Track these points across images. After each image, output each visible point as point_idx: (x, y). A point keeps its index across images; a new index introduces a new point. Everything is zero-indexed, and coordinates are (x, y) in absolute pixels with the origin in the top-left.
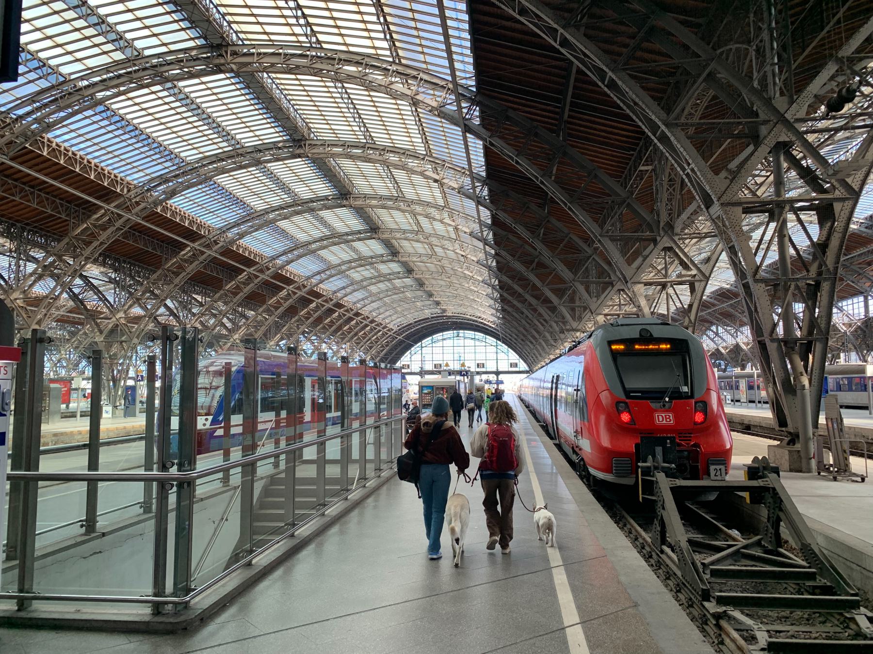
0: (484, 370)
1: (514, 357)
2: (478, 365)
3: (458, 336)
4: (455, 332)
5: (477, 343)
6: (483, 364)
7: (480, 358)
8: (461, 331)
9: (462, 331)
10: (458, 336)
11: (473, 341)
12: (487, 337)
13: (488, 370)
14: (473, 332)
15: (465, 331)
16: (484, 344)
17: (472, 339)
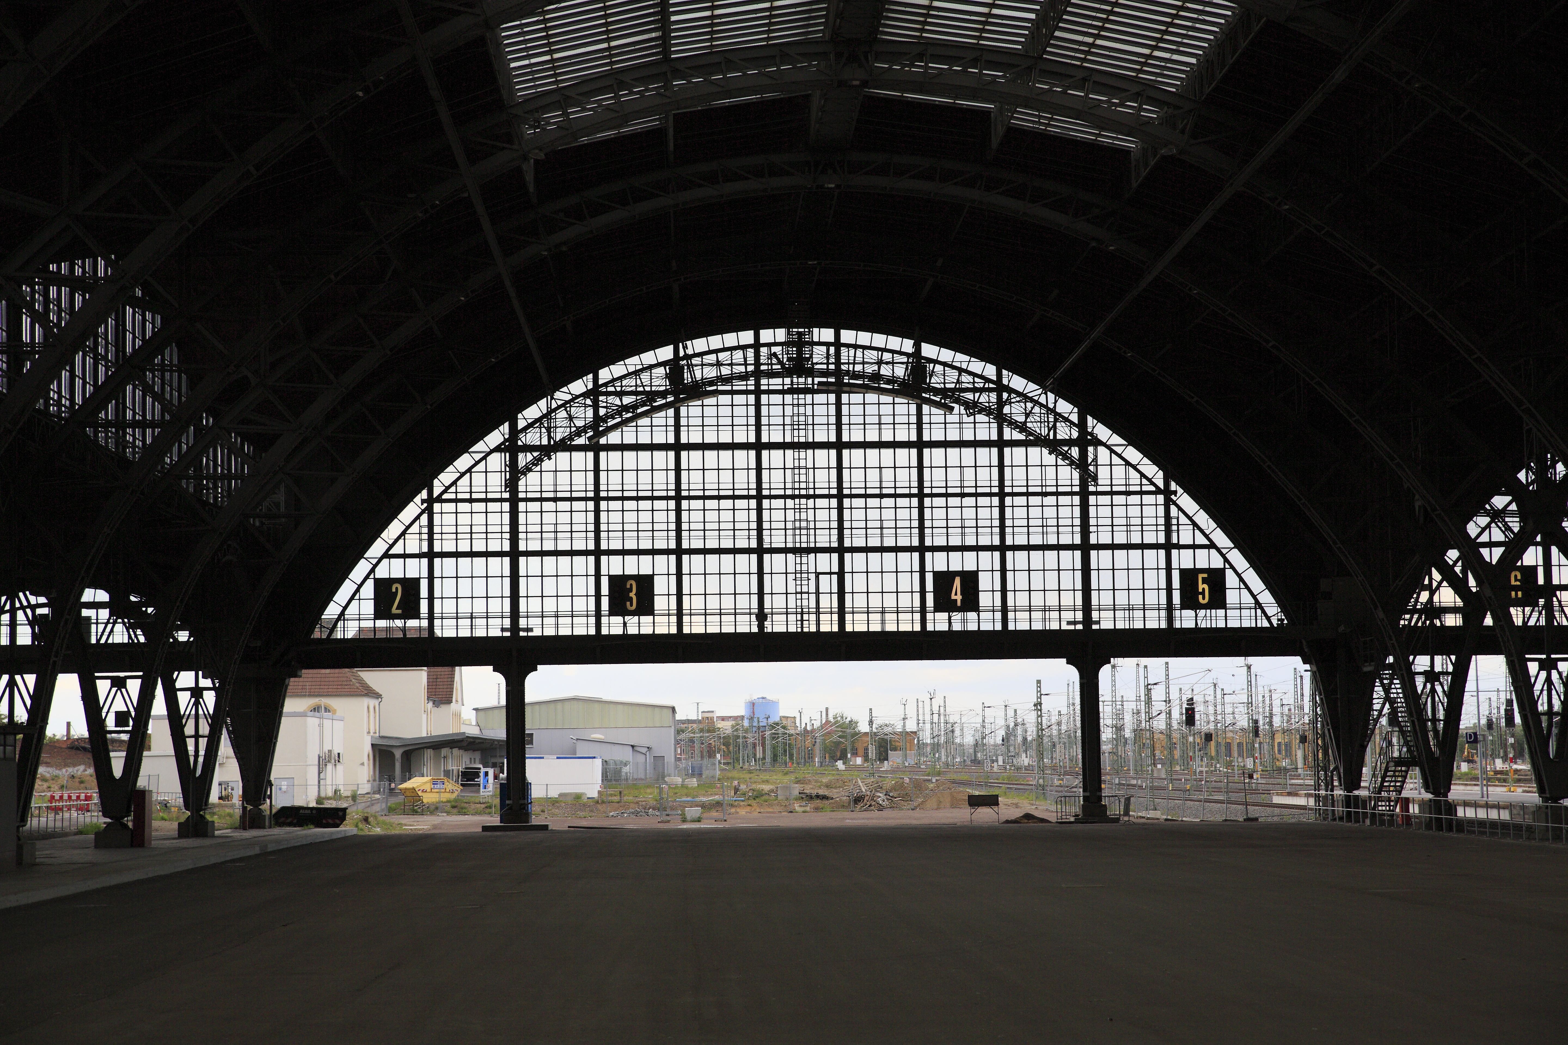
4: (766, 335)
9: (827, 334)
11: (905, 408)
15: (847, 336)
16: (986, 430)
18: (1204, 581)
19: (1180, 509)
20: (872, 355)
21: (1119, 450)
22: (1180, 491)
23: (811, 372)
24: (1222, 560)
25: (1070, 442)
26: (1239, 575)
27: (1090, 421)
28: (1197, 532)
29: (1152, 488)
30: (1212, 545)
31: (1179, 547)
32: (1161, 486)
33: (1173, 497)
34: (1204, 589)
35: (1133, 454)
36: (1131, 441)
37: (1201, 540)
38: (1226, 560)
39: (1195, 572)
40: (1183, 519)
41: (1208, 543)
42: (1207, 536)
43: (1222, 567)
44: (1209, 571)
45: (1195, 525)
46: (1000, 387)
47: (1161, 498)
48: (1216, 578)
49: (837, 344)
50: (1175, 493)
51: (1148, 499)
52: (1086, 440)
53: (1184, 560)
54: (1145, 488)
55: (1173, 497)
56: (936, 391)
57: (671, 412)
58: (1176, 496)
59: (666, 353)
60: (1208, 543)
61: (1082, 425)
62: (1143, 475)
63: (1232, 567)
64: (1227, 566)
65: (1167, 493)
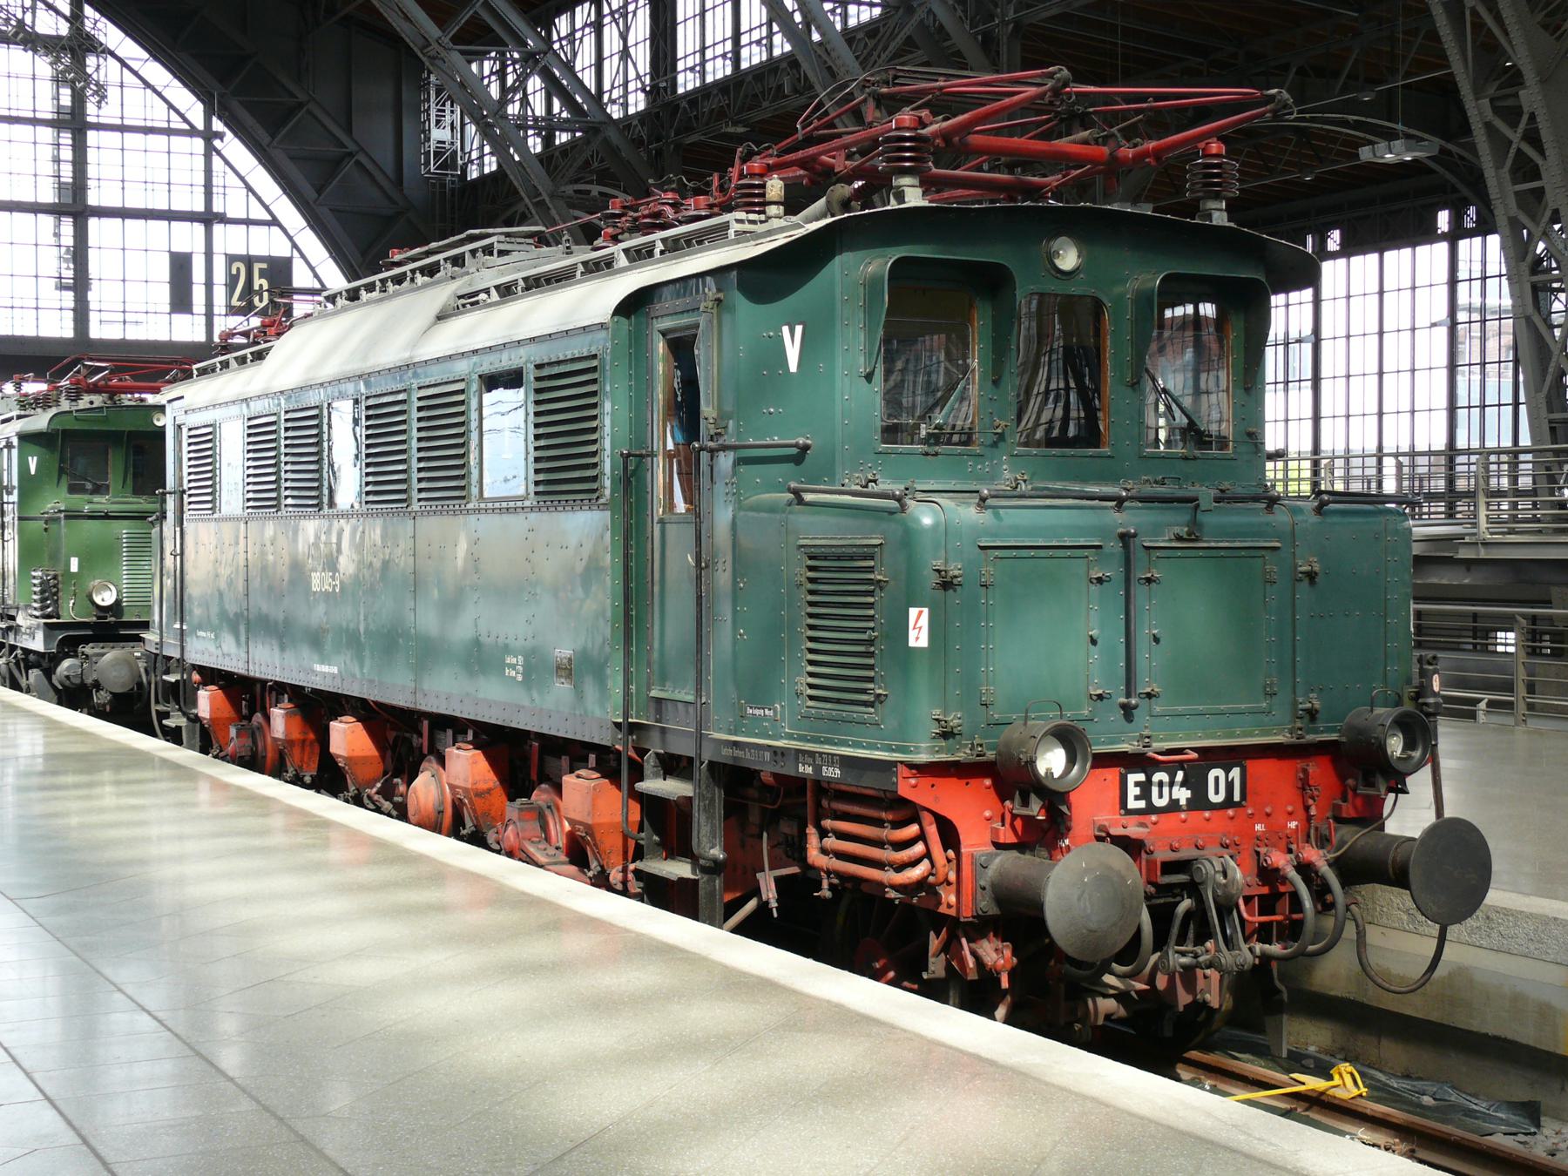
18: (262, 274)
19: (227, 163)
21: (135, 65)
22: (229, 135)
24: (289, 244)
26: (312, 269)
28: (252, 198)
29: (186, 127)
30: (274, 222)
31: (223, 219)
32: (200, 125)
33: (217, 143)
34: (261, 286)
35: (157, 73)
36: (158, 52)
37: (258, 213)
38: (295, 246)
39: (249, 261)
40: (232, 179)
41: (269, 218)
42: (267, 208)
43: (289, 255)
44: (270, 260)
45: (249, 189)
47: (199, 144)
48: (279, 271)
50: (220, 136)
51: (179, 142)
52: (78, 46)
53: (229, 240)
54: (173, 126)
55: (217, 143)
58: (222, 141)
60: (269, 218)
61: (76, 18)
62: (171, 106)
63: (303, 256)
64: (296, 254)
65: (209, 136)
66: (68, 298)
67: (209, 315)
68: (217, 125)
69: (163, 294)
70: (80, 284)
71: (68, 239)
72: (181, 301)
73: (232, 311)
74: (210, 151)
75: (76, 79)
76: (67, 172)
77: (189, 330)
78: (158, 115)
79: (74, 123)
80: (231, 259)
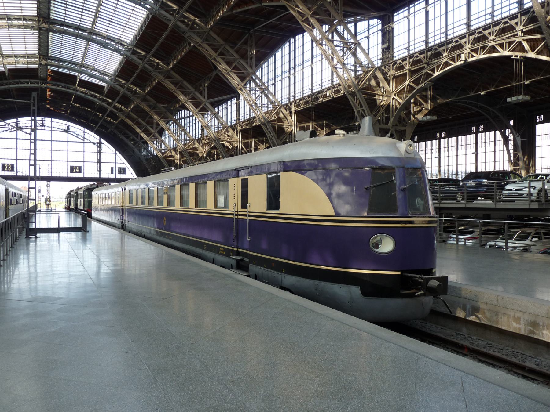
0: (81, 175)
1: (122, 162)
2: (72, 169)
3: (43, 125)
5: (72, 138)
6: (80, 168)
7: (76, 158)
8: (47, 119)
9: (49, 119)
10: (43, 125)
11: (66, 134)
12: (86, 130)
13: (86, 176)
14: (66, 122)
15: (54, 120)
17: (64, 131)
20: (59, 124)
23: (45, 126)
25: (97, 143)
27: (101, 139)
39: (120, 168)
46: (84, 132)
49: (51, 121)
52: (100, 143)
53: (118, 166)
56: (71, 132)
57: (16, 132)
59: (15, 120)
61: (100, 140)
66: (99, 172)
67: (116, 174)
68: (117, 152)
69: (110, 172)
70: (100, 170)
71: (99, 165)
72: (112, 173)
73: (118, 174)
74: (116, 155)
75: (100, 147)
76: (99, 158)
77: (113, 176)
78: (110, 151)
79: (100, 152)
80: (118, 168)
